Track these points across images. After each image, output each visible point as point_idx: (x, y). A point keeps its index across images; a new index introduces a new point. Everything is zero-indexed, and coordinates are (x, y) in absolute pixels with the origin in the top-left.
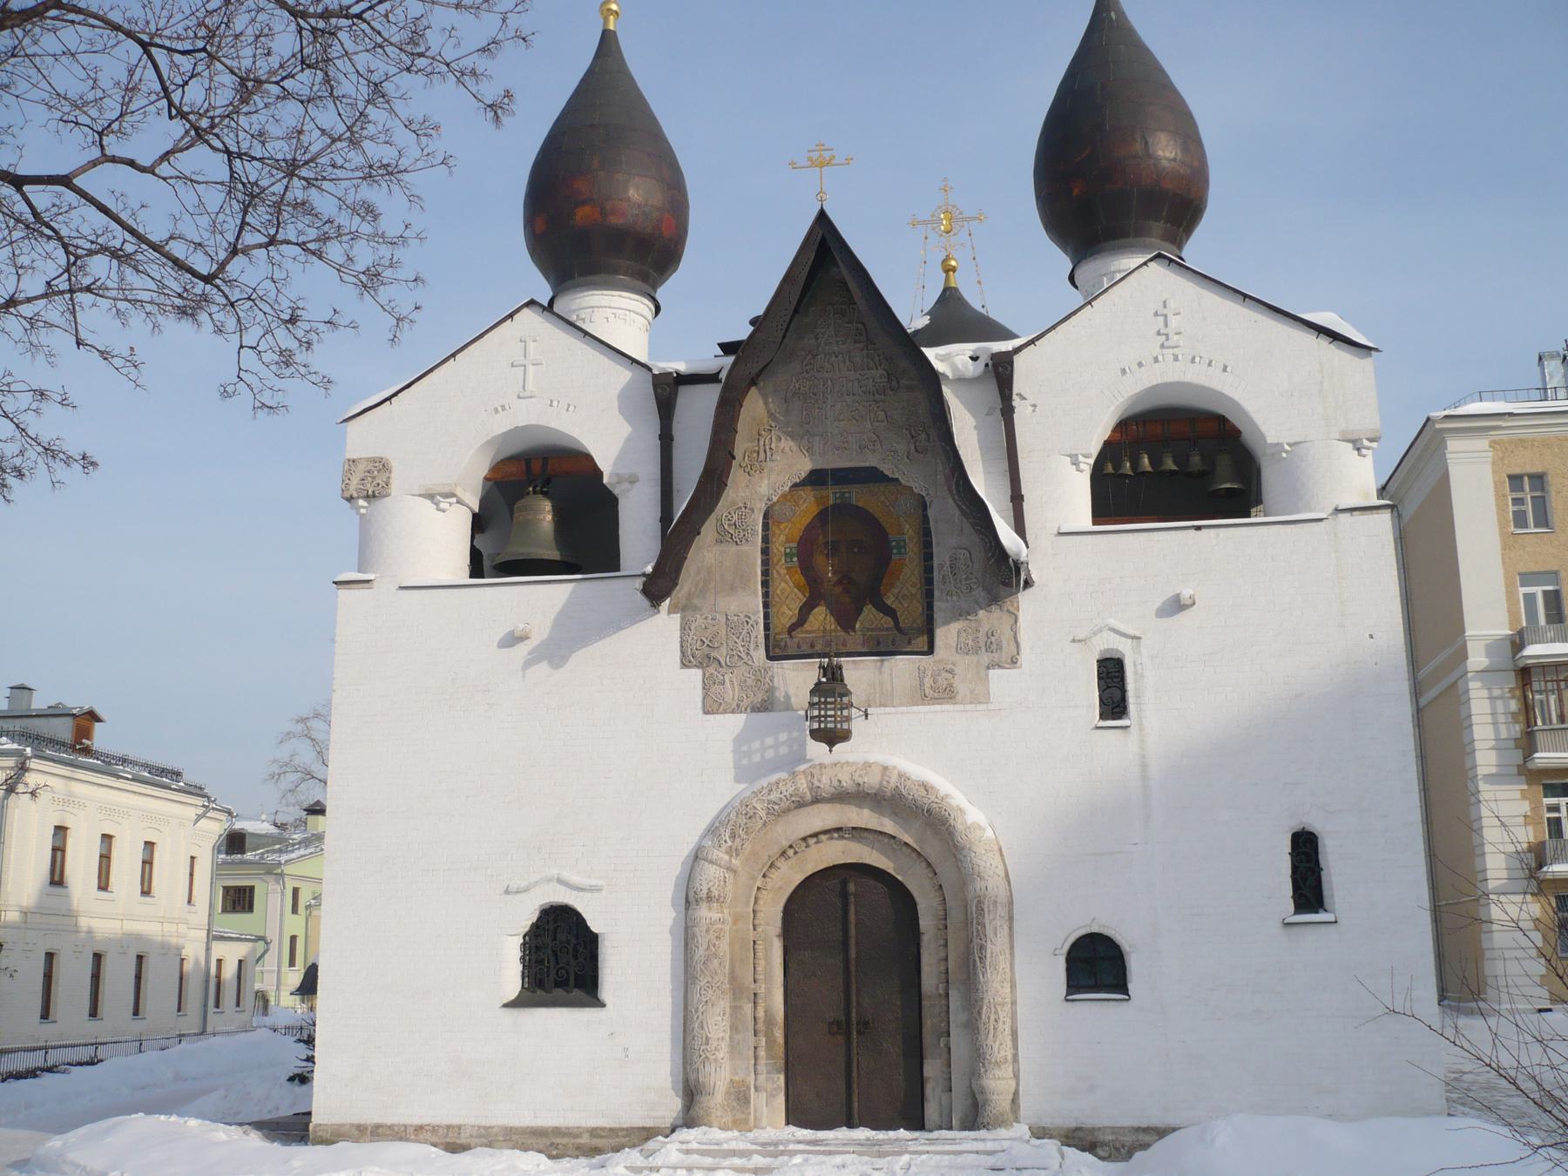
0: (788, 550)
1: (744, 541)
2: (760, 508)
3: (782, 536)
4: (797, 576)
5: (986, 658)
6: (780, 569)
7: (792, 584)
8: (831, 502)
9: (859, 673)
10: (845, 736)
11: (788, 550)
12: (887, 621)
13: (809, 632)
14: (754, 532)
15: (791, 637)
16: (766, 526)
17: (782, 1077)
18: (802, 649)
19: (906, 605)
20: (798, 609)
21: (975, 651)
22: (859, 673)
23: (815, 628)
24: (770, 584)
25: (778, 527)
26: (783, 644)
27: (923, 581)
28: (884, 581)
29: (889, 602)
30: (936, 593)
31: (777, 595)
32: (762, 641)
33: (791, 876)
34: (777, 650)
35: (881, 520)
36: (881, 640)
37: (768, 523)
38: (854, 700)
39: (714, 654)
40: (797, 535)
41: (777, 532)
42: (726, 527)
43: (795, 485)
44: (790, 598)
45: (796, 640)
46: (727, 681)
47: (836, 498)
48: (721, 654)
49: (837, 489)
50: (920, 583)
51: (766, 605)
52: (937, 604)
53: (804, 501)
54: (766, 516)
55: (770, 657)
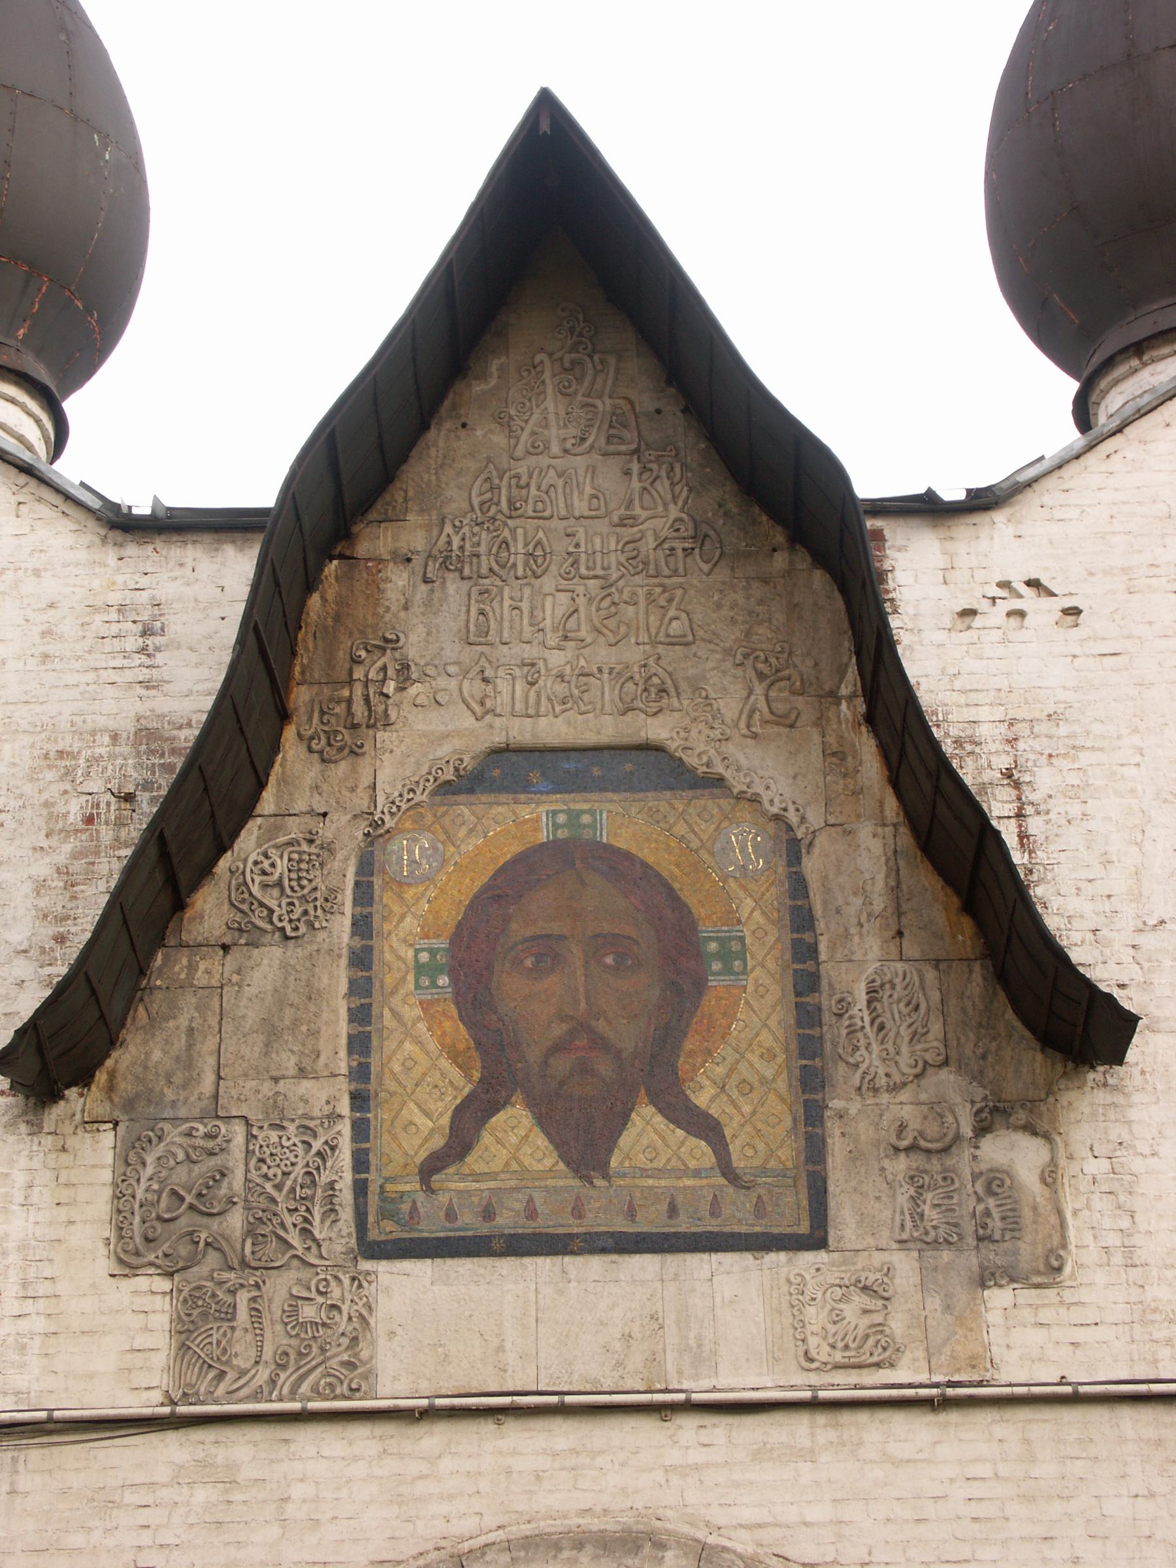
0: (424, 957)
1: (303, 929)
3: (408, 919)
4: (447, 1025)
7: (433, 1045)
8: (543, 836)
11: (424, 957)
12: (700, 1152)
13: (477, 1177)
15: (430, 1190)
16: (364, 893)
18: (459, 1224)
19: (747, 1109)
20: (450, 1113)
23: (496, 1166)
24: (375, 1043)
25: (400, 897)
26: (405, 1207)
27: (794, 1046)
28: (688, 1045)
29: (701, 1100)
31: (392, 1073)
32: (346, 1195)
34: (388, 1225)
35: (676, 886)
36: (680, 1199)
37: (370, 885)
40: (451, 916)
41: (396, 908)
42: (255, 890)
43: (446, 789)
45: (443, 1199)
47: (556, 827)
49: (558, 802)
50: (786, 1050)
51: (359, 1100)
53: (471, 831)
54: (366, 866)
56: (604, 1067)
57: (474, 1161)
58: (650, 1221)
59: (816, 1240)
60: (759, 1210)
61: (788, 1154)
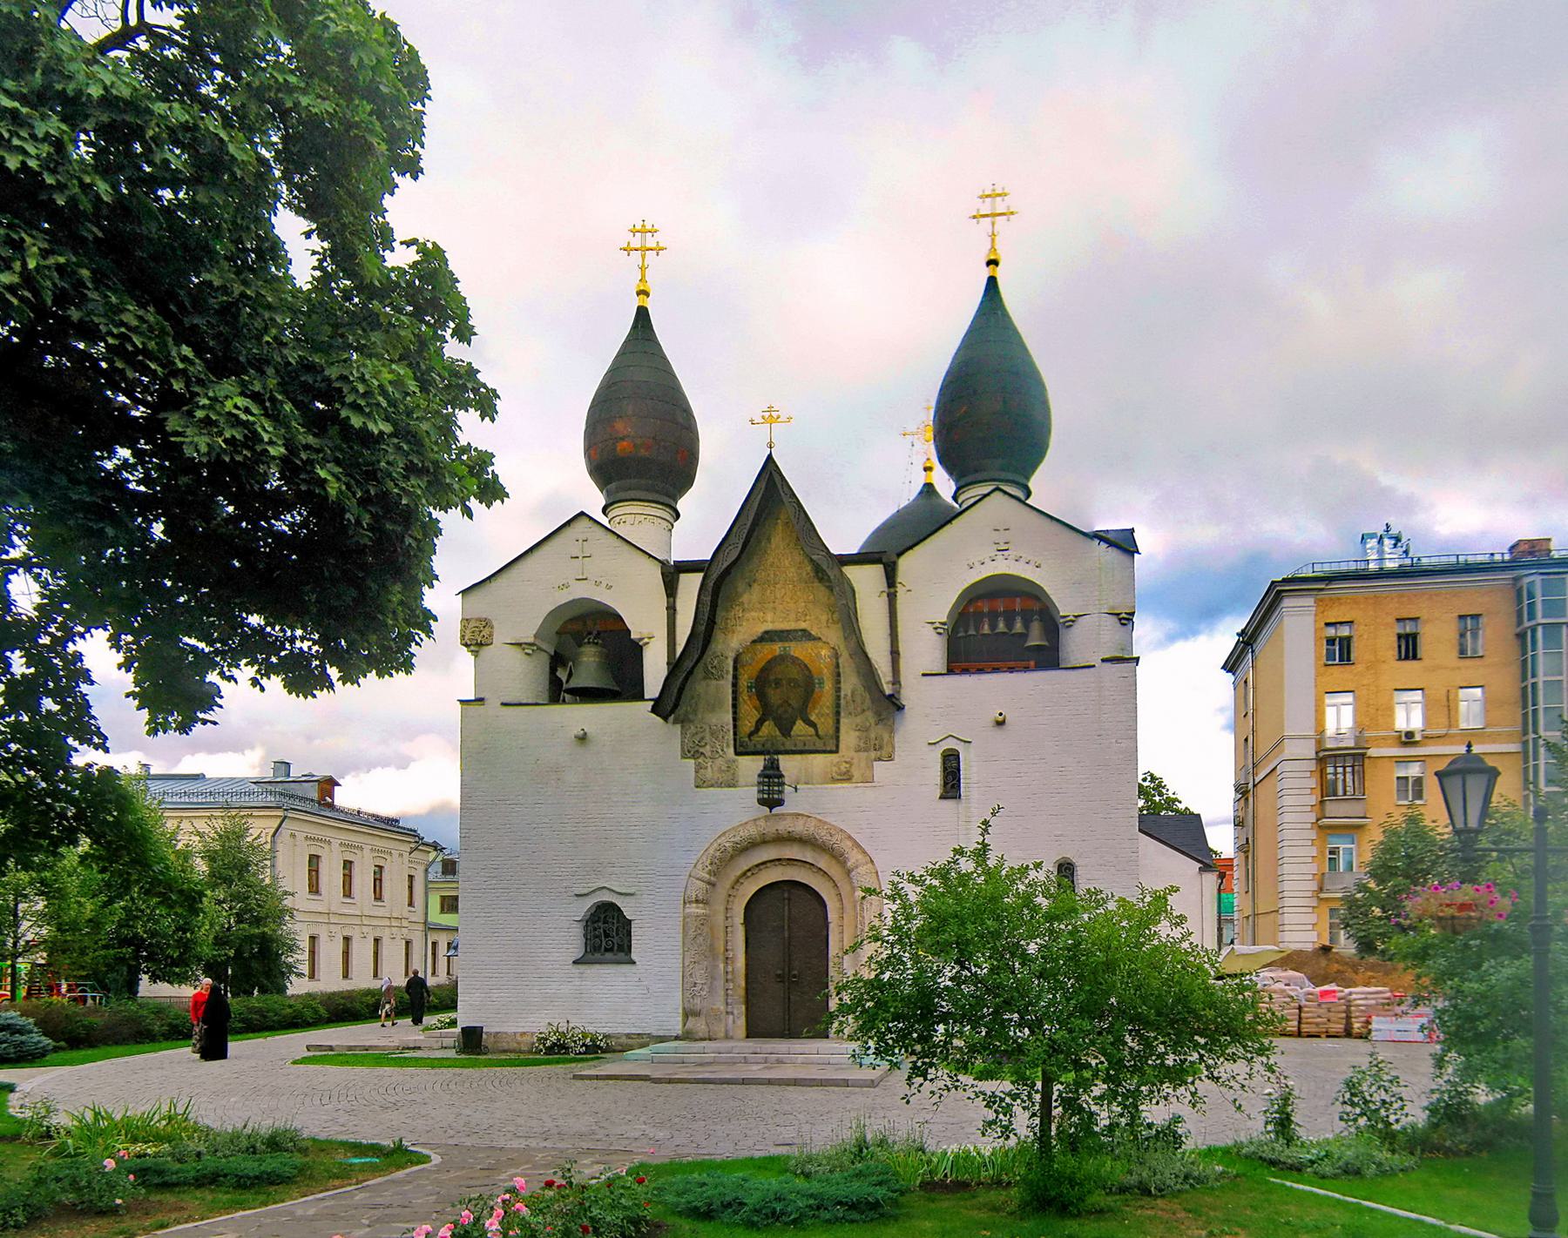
2: (731, 655)
5: (873, 754)
6: (744, 695)
8: (777, 653)
9: (788, 764)
10: (780, 803)
12: (811, 731)
14: (728, 672)
15: (750, 740)
16: (735, 669)
17: (744, 1007)
21: (866, 750)
22: (788, 764)
28: (810, 705)
29: (813, 718)
30: (842, 714)
32: (732, 742)
33: (751, 888)
38: (786, 780)
39: (701, 750)
40: (755, 674)
43: (754, 642)
44: (750, 714)
46: (709, 769)
48: (707, 750)
49: (780, 644)
51: (735, 719)
52: (842, 720)
54: (736, 661)
55: (737, 753)
56: (790, 710)
57: (760, 734)
58: (800, 747)
59: (836, 752)
60: (825, 745)
61: (831, 732)
